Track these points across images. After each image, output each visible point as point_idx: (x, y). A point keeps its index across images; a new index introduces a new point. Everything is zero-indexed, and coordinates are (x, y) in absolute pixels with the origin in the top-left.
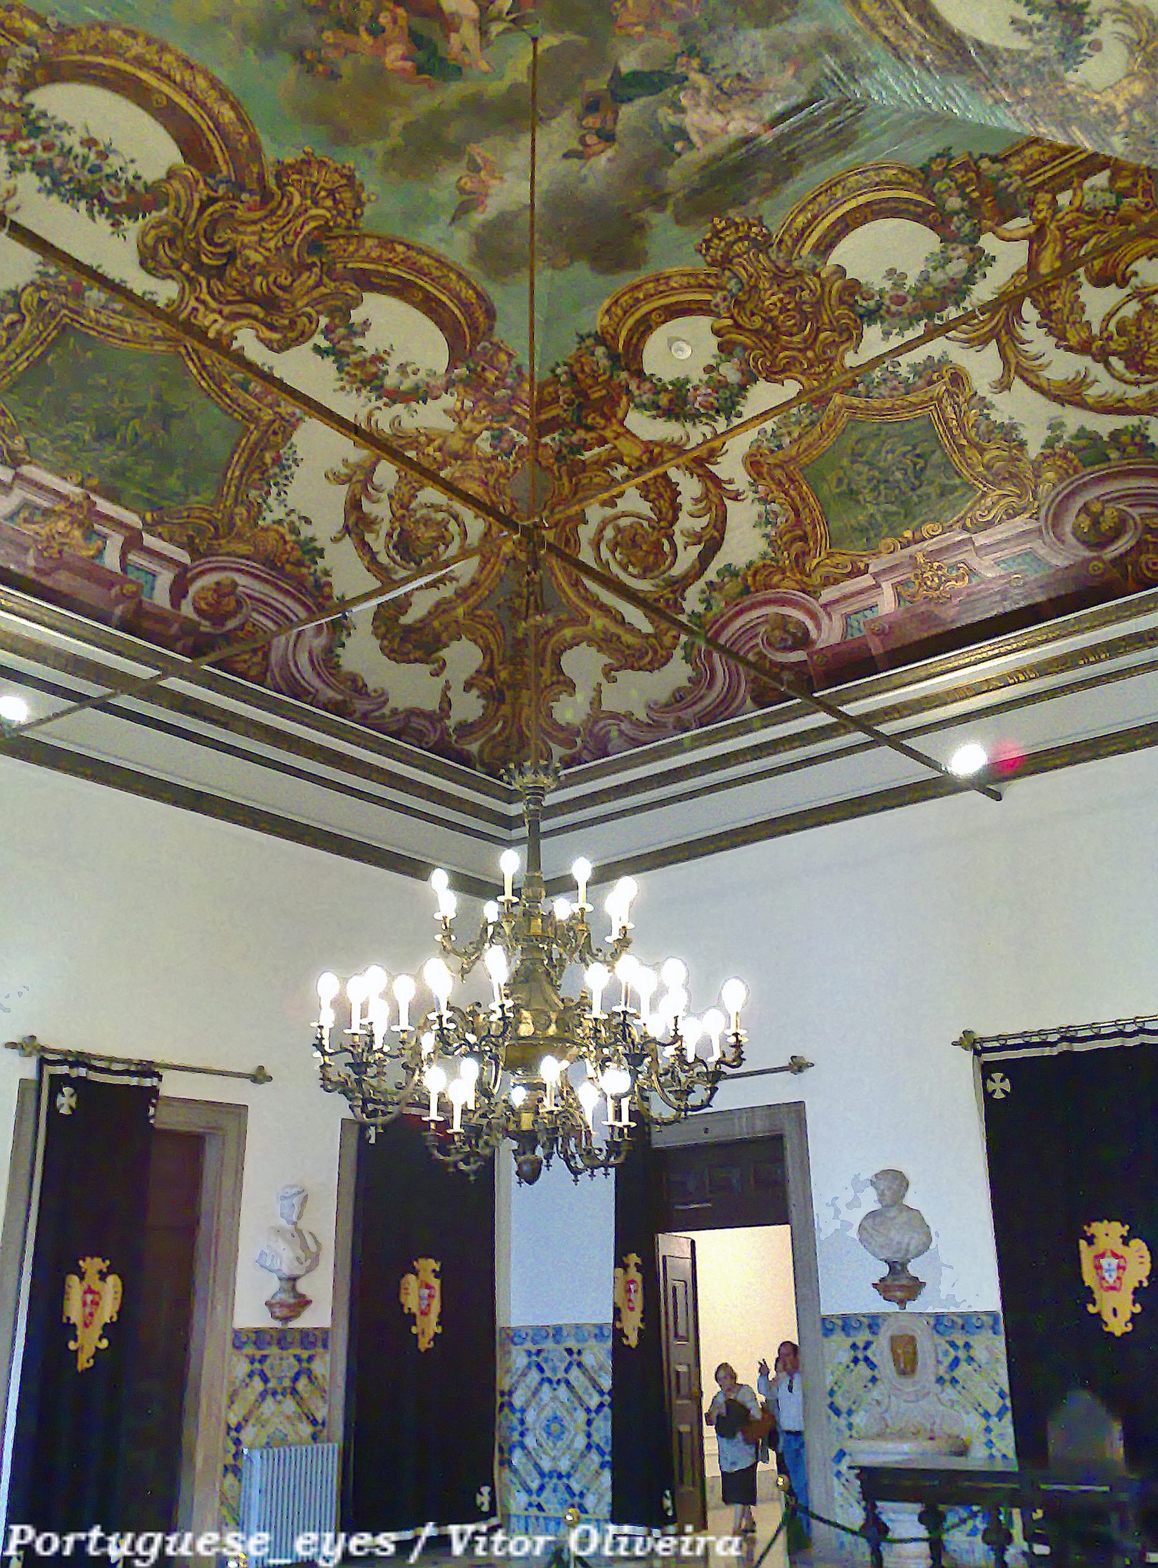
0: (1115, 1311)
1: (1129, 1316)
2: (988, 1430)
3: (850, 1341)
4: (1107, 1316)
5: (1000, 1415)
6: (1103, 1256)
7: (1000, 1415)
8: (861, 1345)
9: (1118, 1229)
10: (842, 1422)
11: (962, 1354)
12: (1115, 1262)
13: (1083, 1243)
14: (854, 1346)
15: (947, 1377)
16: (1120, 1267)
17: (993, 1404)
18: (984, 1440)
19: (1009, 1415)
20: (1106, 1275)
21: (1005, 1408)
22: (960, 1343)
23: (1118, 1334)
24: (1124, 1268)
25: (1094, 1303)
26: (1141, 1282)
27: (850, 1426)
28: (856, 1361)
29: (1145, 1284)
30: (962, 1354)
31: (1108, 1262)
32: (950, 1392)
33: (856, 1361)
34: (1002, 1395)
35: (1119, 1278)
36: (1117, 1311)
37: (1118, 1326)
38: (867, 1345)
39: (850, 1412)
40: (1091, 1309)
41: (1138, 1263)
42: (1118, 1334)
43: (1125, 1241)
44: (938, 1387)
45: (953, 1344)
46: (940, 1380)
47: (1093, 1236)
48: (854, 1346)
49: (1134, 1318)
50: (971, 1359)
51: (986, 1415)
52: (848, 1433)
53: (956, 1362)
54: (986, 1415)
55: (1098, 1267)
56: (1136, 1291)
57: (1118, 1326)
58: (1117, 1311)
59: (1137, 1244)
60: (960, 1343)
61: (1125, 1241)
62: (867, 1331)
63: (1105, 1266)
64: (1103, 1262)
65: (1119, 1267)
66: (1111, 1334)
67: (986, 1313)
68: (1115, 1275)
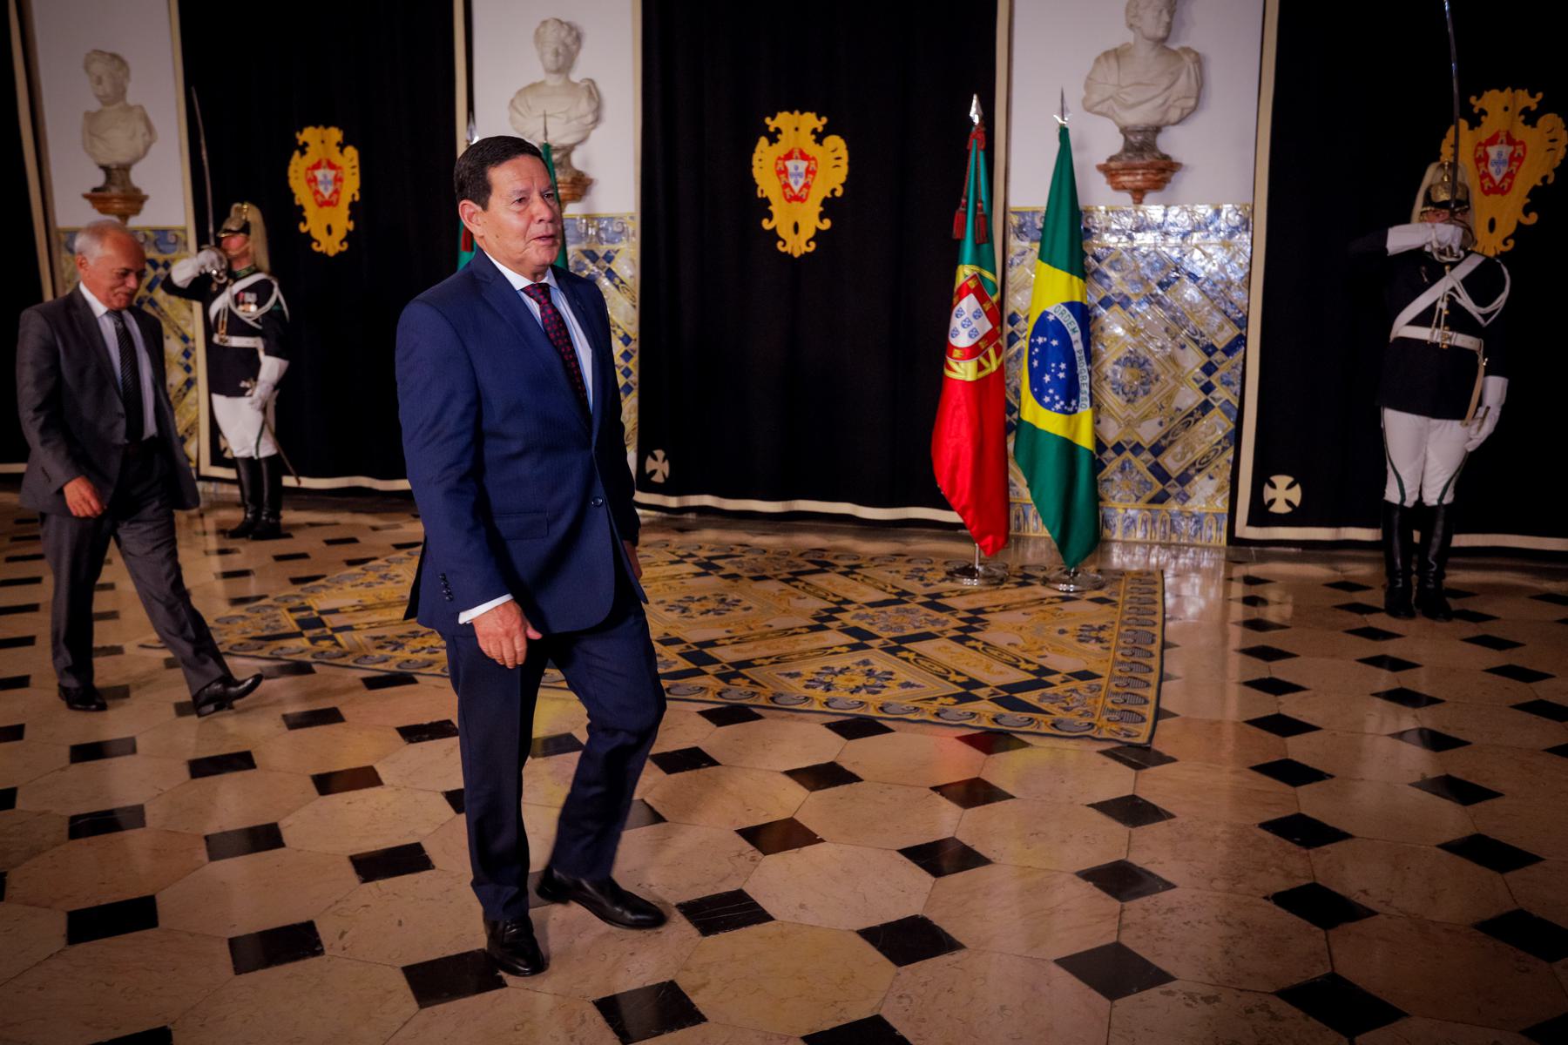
0: (796, 228)
1: (811, 233)
4: (785, 231)
6: (789, 156)
9: (811, 121)
12: (803, 165)
13: (763, 141)
20: (791, 181)
23: (796, 255)
24: (814, 173)
25: (770, 216)
26: (833, 191)
29: (839, 193)
35: (807, 186)
36: (796, 225)
40: (767, 225)
41: (831, 165)
43: (819, 138)
47: (778, 131)
49: (819, 236)
56: (826, 203)
58: (796, 225)
59: (836, 143)
61: (819, 138)
63: (791, 169)
64: (790, 164)
65: (808, 171)
68: (801, 181)
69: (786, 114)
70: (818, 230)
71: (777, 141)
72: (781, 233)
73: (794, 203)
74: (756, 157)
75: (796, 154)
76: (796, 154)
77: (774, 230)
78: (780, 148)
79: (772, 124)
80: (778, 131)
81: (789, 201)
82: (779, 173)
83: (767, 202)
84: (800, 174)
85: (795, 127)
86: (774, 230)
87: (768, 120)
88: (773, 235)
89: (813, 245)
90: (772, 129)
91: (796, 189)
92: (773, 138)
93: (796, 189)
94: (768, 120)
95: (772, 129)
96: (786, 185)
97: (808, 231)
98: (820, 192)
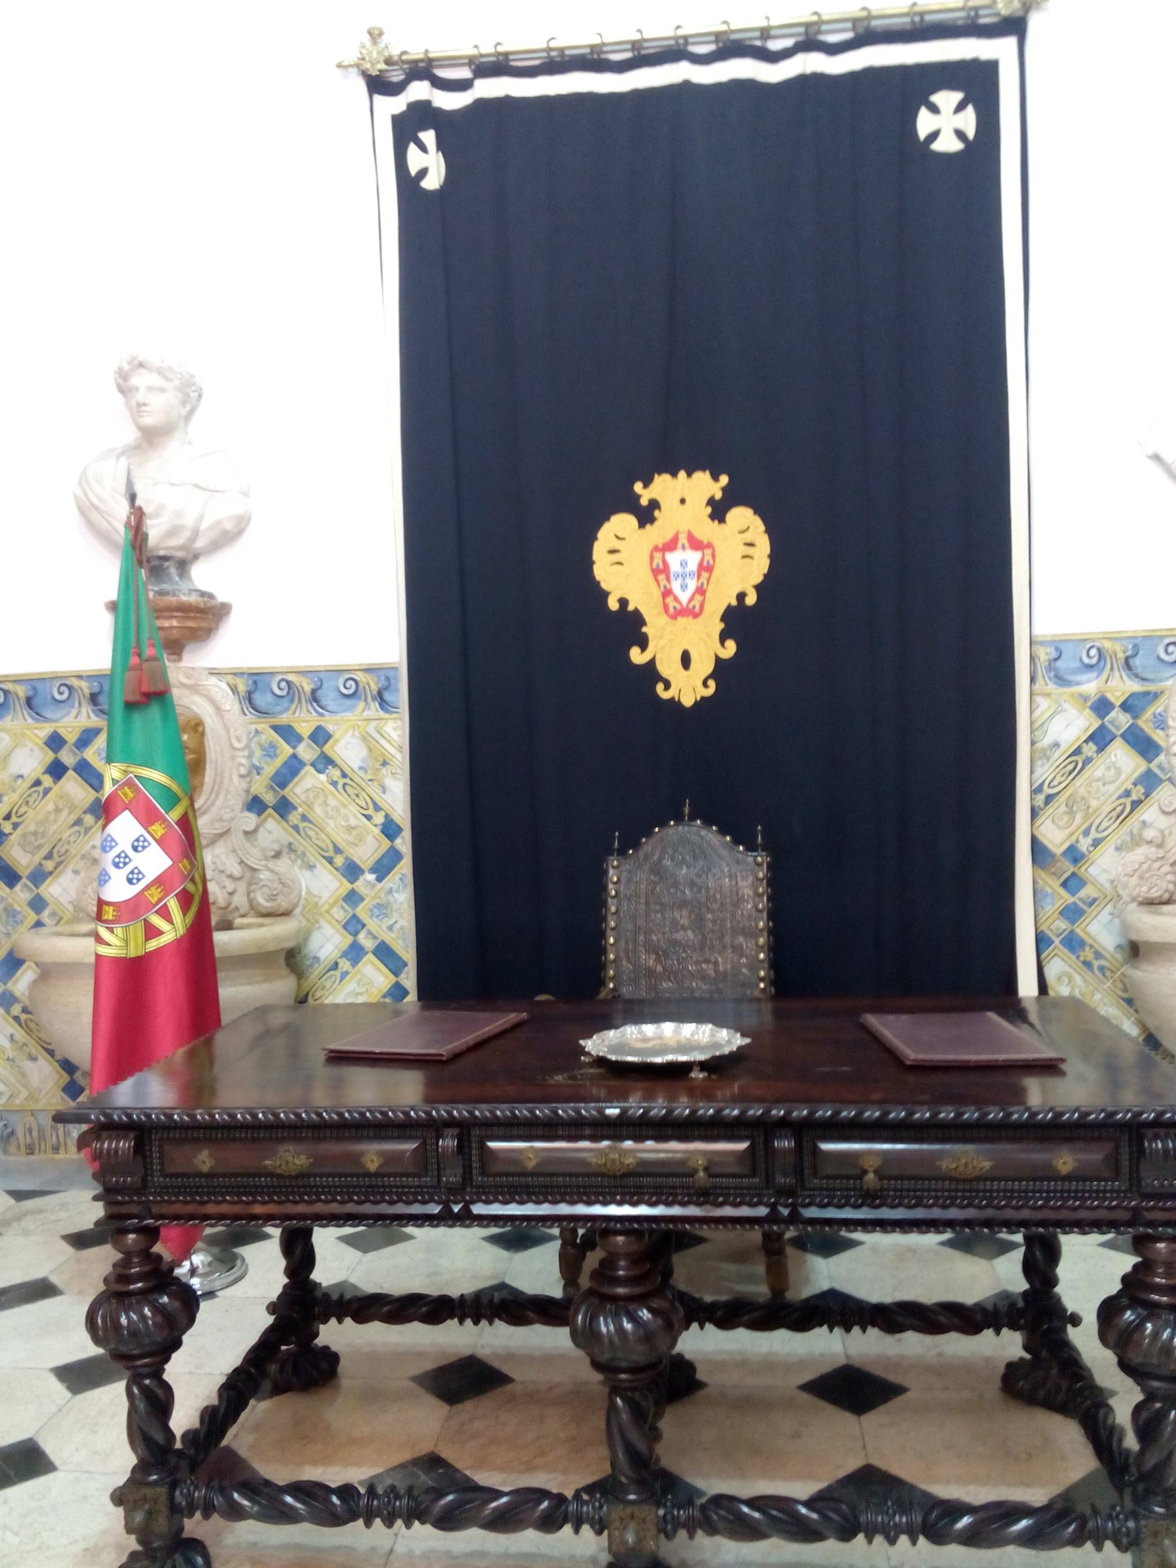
0: (686, 660)
1: (709, 668)
2: (353, 898)
3: (45, 730)
4: (668, 667)
5: (382, 869)
6: (671, 546)
7: (382, 869)
8: (71, 737)
10: (21, 895)
11: (306, 751)
12: (693, 558)
14: (55, 742)
15: (269, 798)
16: (705, 568)
17: (368, 848)
18: (340, 914)
19: (405, 867)
20: (676, 586)
21: (393, 857)
22: (305, 730)
23: (688, 701)
24: (710, 569)
25: (643, 644)
27: (38, 904)
28: (57, 770)
30: (306, 751)
31: (684, 560)
32: (273, 830)
33: (57, 770)
34: (390, 830)
35: (701, 591)
37: (688, 687)
38: (86, 738)
39: (39, 877)
40: (637, 656)
42: (688, 701)
44: (251, 820)
45: (287, 733)
46: (256, 805)
48: (55, 742)
49: (721, 669)
50: (325, 762)
51: (352, 871)
52: (32, 917)
53: (293, 768)
54: (352, 871)
55: (660, 571)
57: (688, 687)
60: (305, 730)
62: (87, 709)
64: (674, 559)
66: (674, 704)
67: (369, 670)
68: (692, 585)
69: (666, 477)
70: (718, 660)
71: (652, 520)
72: (663, 669)
73: (682, 621)
74: (599, 551)
75: (683, 539)
76: (683, 539)
77: (652, 662)
78: (657, 533)
79: (644, 494)
80: (654, 504)
81: (674, 617)
82: (656, 572)
83: (637, 619)
84: (681, 569)
85: (682, 495)
86: (652, 662)
87: (638, 487)
88: (650, 672)
89: (712, 684)
90: (644, 502)
91: (684, 597)
92: (646, 515)
93: (684, 597)
94: (638, 487)
95: (644, 502)
96: (667, 593)
97: (703, 666)
98: (721, 598)
